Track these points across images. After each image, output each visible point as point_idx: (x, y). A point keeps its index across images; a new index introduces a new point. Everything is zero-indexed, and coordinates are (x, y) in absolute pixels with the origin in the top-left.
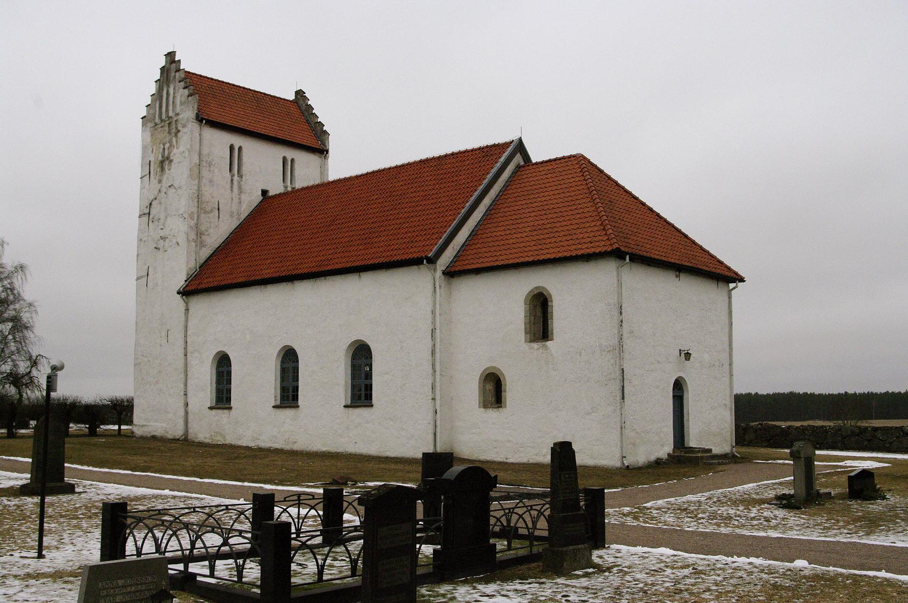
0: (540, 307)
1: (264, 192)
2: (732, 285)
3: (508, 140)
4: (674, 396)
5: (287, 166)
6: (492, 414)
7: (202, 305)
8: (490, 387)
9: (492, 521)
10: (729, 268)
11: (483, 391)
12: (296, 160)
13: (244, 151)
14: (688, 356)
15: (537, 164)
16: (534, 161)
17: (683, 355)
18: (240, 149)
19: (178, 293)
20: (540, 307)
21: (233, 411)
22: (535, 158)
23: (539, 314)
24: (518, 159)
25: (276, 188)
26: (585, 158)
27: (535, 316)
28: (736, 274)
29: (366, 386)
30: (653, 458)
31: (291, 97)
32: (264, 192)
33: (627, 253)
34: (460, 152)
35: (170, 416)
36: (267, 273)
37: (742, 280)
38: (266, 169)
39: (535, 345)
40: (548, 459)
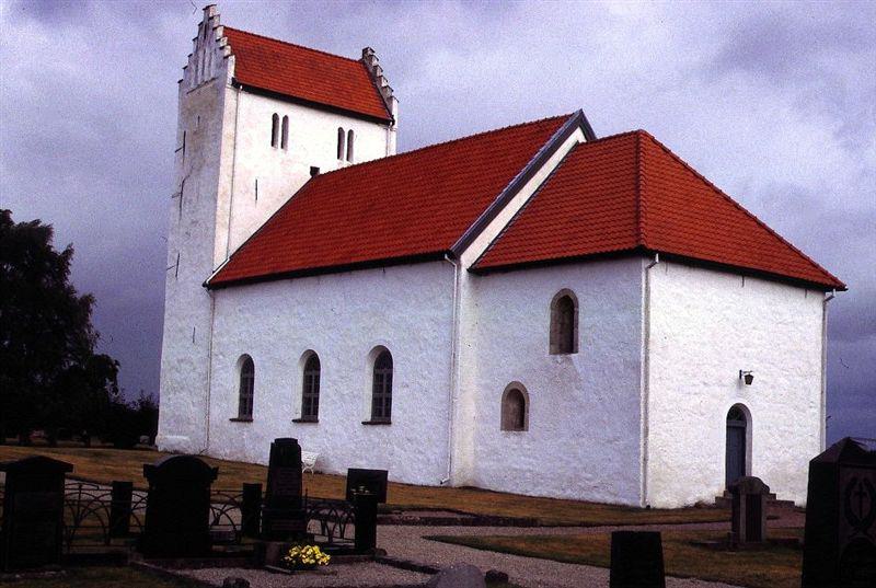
0: (566, 309)
1: (314, 170)
2: (828, 294)
3: (570, 113)
4: (728, 427)
5: (344, 141)
6: (513, 438)
7: (229, 301)
8: (514, 406)
9: (133, 521)
10: (825, 273)
11: (496, 405)
12: (355, 133)
13: (290, 120)
14: (749, 379)
15: (601, 140)
16: (599, 137)
17: (743, 377)
18: (286, 119)
19: (204, 286)
20: (566, 309)
21: (254, 424)
22: (601, 132)
23: (567, 321)
24: (578, 136)
25: (329, 163)
26: (646, 135)
27: (562, 324)
28: (835, 280)
29: (310, 391)
30: (691, 501)
31: (358, 56)
32: (314, 170)
33: (657, 251)
34: (517, 126)
35: (193, 428)
36: (294, 265)
37: (841, 288)
38: (316, 142)
39: (559, 358)
40: (265, 460)
